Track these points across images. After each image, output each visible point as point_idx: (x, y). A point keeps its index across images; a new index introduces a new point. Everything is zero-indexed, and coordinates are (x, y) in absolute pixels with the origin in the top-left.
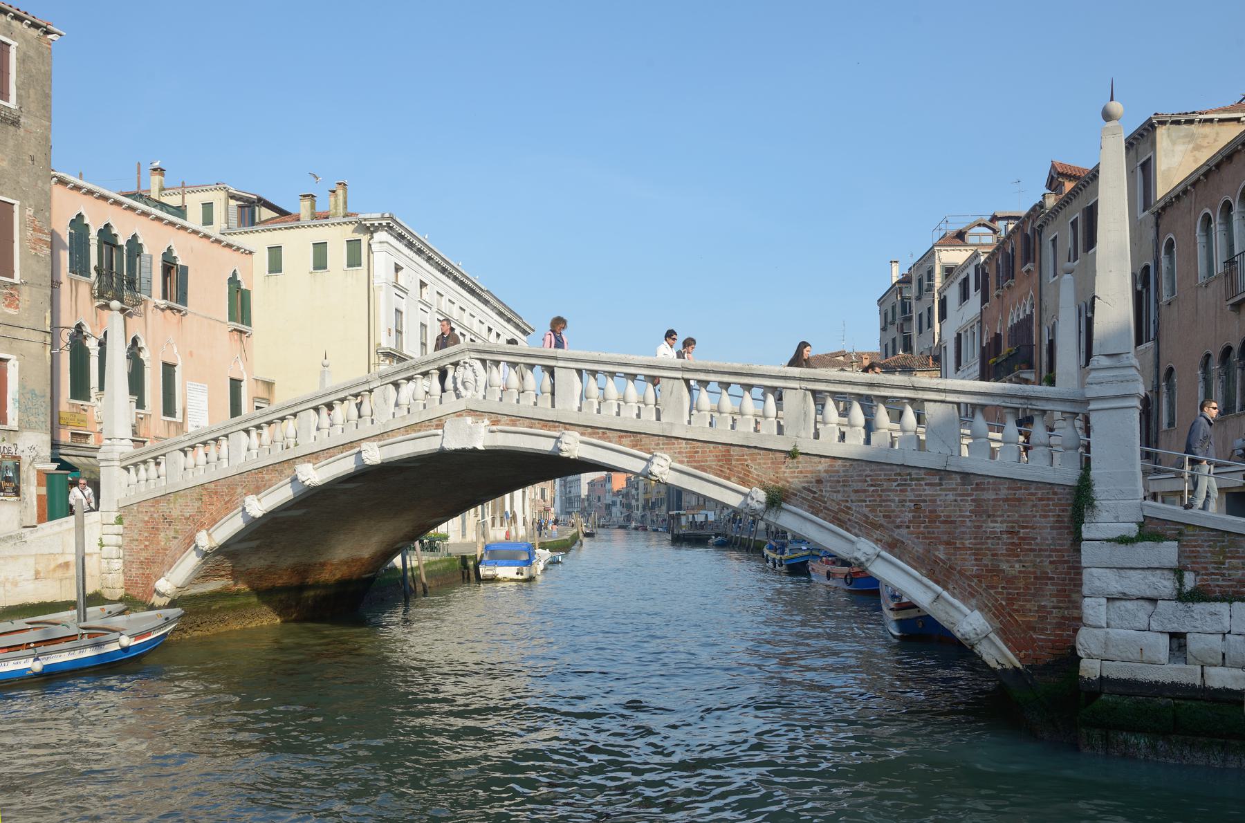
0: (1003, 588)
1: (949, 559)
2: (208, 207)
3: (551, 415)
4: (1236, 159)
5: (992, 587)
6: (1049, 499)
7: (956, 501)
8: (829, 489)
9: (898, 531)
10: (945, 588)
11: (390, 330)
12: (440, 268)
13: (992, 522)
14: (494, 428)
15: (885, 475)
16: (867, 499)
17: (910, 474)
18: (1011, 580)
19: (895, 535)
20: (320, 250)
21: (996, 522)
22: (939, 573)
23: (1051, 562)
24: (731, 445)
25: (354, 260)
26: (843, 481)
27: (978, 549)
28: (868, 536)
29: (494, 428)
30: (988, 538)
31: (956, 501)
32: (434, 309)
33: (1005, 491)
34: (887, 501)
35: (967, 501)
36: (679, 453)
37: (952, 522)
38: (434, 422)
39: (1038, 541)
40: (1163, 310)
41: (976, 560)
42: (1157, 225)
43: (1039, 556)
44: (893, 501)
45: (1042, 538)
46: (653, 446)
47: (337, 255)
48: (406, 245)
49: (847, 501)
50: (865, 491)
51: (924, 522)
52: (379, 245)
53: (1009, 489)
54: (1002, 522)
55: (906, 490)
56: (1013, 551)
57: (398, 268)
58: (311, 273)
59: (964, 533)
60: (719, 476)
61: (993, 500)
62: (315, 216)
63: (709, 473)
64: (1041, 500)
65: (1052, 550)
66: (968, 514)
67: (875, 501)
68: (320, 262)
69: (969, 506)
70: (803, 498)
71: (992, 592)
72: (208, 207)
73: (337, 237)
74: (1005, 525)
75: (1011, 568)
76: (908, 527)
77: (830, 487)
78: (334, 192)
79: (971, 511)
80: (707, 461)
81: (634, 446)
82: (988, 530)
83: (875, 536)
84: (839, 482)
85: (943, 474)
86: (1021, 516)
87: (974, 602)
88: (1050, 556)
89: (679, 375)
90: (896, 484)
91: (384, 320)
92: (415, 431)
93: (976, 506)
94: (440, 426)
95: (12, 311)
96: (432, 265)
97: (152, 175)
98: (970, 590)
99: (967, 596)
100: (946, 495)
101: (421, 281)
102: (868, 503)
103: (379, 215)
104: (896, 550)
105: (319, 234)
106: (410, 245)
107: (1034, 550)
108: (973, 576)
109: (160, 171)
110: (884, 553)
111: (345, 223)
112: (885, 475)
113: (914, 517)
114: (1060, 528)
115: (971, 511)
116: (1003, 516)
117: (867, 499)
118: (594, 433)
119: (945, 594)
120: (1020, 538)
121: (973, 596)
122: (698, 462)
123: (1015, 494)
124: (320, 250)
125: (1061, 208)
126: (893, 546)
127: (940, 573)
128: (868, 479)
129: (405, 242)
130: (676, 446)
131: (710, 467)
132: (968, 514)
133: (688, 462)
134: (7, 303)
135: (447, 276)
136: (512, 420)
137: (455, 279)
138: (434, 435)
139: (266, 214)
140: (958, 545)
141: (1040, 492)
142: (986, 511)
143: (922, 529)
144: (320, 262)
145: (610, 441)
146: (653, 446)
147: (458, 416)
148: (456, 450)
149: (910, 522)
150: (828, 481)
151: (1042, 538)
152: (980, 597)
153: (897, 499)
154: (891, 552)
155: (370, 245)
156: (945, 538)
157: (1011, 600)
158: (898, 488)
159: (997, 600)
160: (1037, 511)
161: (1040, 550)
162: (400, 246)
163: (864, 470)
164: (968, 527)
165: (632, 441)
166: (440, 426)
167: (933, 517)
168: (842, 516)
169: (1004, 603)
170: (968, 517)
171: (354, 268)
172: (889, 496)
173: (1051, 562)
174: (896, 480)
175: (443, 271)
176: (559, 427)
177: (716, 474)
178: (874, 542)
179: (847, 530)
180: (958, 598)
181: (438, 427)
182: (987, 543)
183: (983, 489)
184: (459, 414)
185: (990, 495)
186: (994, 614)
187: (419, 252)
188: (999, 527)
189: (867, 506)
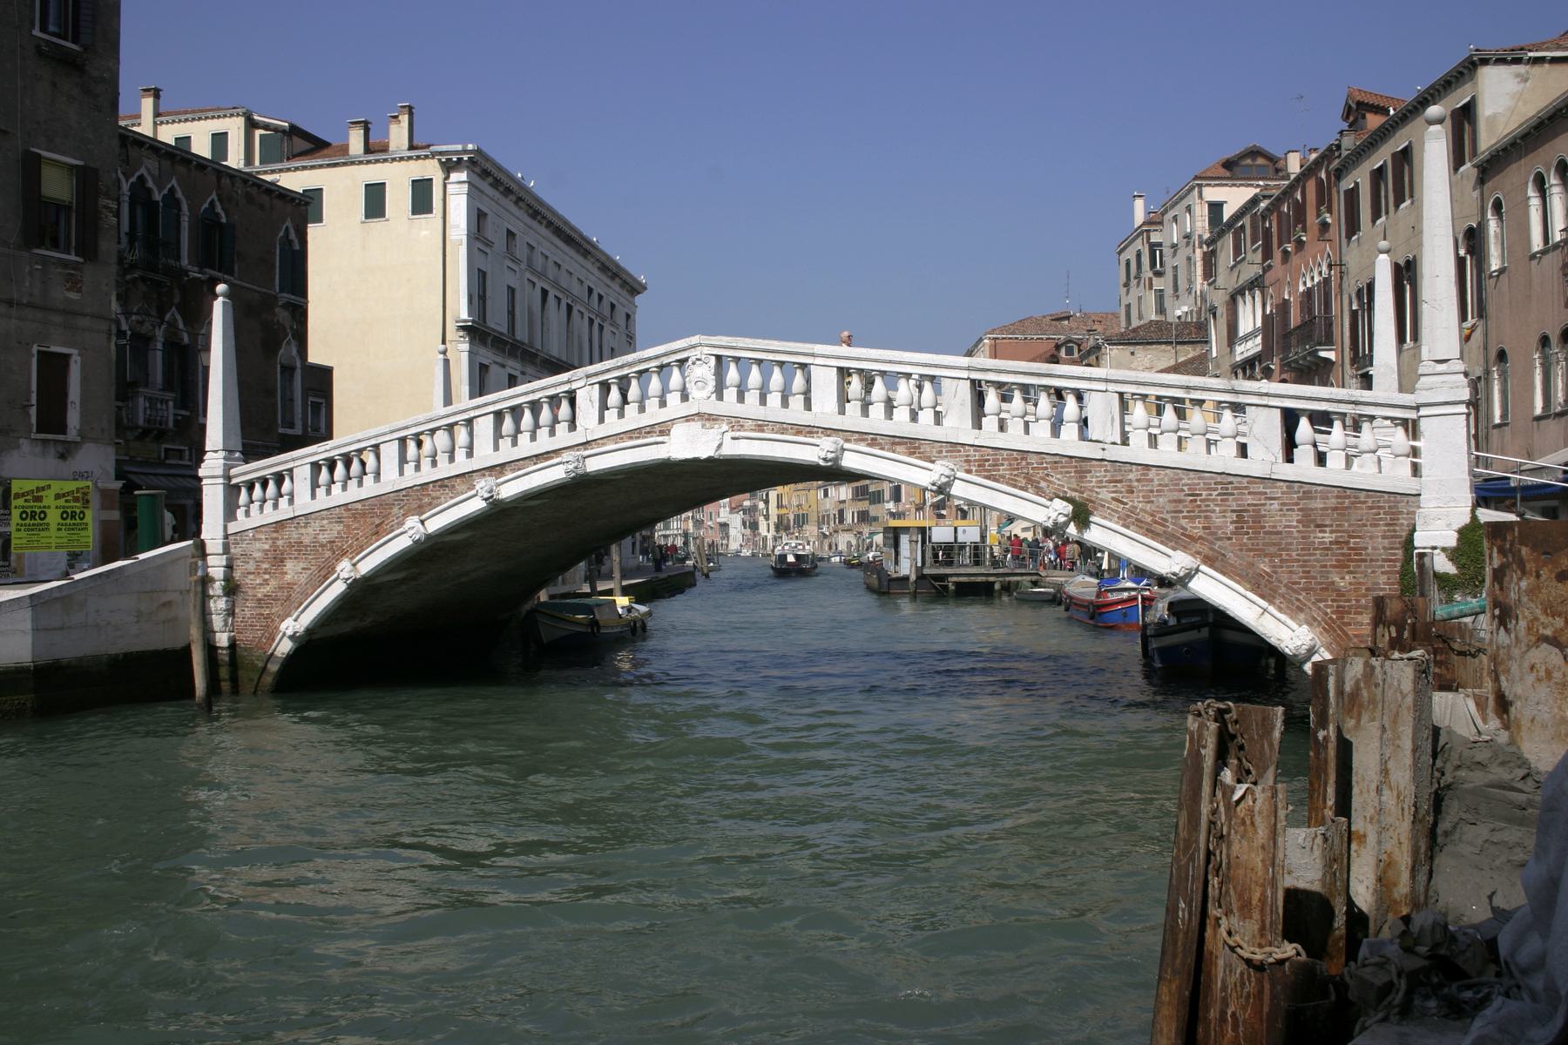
0: (1332, 601)
1: (1275, 572)
3: (805, 418)
5: (1320, 601)
6: (1379, 507)
7: (1281, 510)
8: (1141, 499)
9: (1219, 543)
10: (1271, 602)
12: (530, 211)
13: (1320, 532)
14: (737, 434)
15: (1204, 484)
16: (1185, 510)
17: (1231, 483)
19: (1216, 547)
21: (1325, 532)
22: (1262, 586)
23: (1382, 573)
24: (1028, 452)
26: (1157, 491)
27: (1304, 561)
28: (1185, 548)
29: (737, 434)
30: (1315, 549)
31: (1281, 510)
33: (1333, 500)
34: (1207, 511)
35: (1293, 510)
36: (968, 461)
37: (1280, 533)
38: (657, 428)
39: (1369, 551)
41: (1304, 572)
43: (1370, 567)
44: (1214, 511)
45: (1374, 548)
46: (935, 454)
47: (398, 199)
48: (491, 185)
49: (1162, 513)
50: (1180, 501)
51: (1248, 533)
53: (1338, 497)
54: (1332, 532)
55: (1227, 500)
56: (1341, 566)
58: (363, 223)
59: (1291, 544)
60: (1015, 486)
61: (1322, 509)
62: (368, 150)
63: (1002, 483)
64: (1371, 508)
65: (1384, 560)
66: (1295, 524)
67: (1193, 512)
69: (1295, 517)
70: (1113, 510)
71: (1322, 605)
73: (398, 178)
74: (1334, 535)
76: (1230, 539)
77: (1143, 497)
78: (396, 117)
79: (1298, 521)
80: (999, 470)
81: (911, 454)
82: (1316, 540)
83: (1194, 550)
84: (1152, 491)
86: (1350, 525)
87: (1302, 616)
88: (1383, 566)
89: (965, 374)
90: (1216, 493)
92: (631, 438)
93: (1303, 516)
95: (73, 296)
96: (520, 208)
97: (143, 97)
98: (1297, 603)
99: (1294, 609)
100: (1271, 504)
101: (508, 231)
102: (1185, 514)
103: (459, 147)
104: (1217, 564)
105: (374, 173)
107: (1365, 561)
108: (1304, 589)
109: (157, 94)
110: (1203, 568)
112: (1204, 484)
113: (1236, 528)
114: (1392, 537)
115: (1298, 521)
116: (1331, 526)
117: (1185, 510)
118: (862, 440)
119: (1271, 609)
120: (1350, 549)
121: (1301, 610)
122: (989, 471)
123: (1344, 503)
125: (1363, 150)
127: (1266, 586)
128: (1185, 488)
129: (490, 180)
130: (962, 453)
131: (1003, 477)
132: (1295, 524)
133: (976, 471)
134: (68, 285)
136: (760, 426)
137: (550, 224)
138: (657, 443)
140: (1284, 557)
141: (1370, 500)
142: (1314, 521)
143: (1245, 541)
145: (882, 449)
146: (935, 454)
147: (687, 421)
148: (686, 461)
149: (1232, 533)
150: (1140, 491)
151: (1374, 548)
152: (1308, 610)
153: (1217, 509)
154: (1211, 566)
156: (1272, 549)
157: (1341, 612)
158: (1219, 498)
159: (1326, 614)
160: (1367, 520)
161: (1372, 560)
163: (1181, 479)
164: (1295, 538)
165: (908, 449)
168: (1159, 528)
169: (1334, 617)
170: (1295, 527)
172: (1209, 506)
173: (1382, 573)
174: (1215, 490)
176: (817, 433)
177: (1008, 484)
178: (1191, 555)
179: (1162, 543)
180: (1285, 613)
181: (662, 433)
182: (1315, 554)
183: (1311, 498)
184: (688, 418)
186: (1324, 628)
187: (508, 191)
189: (1184, 517)
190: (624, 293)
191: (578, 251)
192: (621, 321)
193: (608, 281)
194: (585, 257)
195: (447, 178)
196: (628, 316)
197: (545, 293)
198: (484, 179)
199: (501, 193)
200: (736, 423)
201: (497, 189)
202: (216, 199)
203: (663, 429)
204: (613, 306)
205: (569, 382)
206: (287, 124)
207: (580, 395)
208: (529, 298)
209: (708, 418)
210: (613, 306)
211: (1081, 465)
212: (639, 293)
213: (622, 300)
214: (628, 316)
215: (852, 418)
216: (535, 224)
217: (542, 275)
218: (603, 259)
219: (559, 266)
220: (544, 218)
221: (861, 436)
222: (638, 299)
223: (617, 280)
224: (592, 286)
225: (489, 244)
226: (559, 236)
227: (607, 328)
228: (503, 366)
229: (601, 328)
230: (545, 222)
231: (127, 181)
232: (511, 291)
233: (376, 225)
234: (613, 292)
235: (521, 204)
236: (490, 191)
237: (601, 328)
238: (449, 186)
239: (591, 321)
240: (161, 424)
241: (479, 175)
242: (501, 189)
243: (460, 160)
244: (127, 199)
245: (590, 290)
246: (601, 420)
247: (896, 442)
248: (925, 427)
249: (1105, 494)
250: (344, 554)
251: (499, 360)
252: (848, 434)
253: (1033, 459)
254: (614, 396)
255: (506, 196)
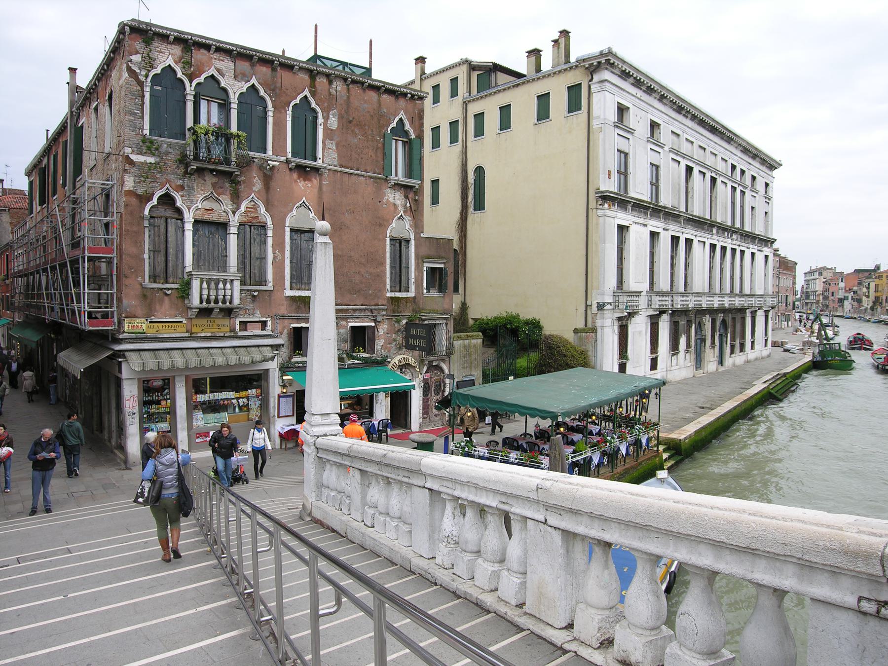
2: (454, 81)
11: (609, 172)
20: (544, 99)
25: (574, 105)
32: (666, 148)
48: (633, 84)
52: (597, 85)
57: (622, 110)
58: (536, 124)
68: (543, 114)
72: (454, 81)
91: (608, 161)
96: (666, 104)
105: (540, 88)
106: (638, 83)
111: (565, 70)
124: (544, 99)
129: (631, 80)
135: (684, 115)
137: (694, 118)
139: (502, 78)
144: (543, 114)
155: (589, 87)
162: (626, 85)
171: (574, 113)
175: (680, 110)
187: (650, 90)
190: (764, 168)
191: (722, 139)
192: (760, 186)
193: (750, 161)
194: (729, 143)
195: (591, 80)
196: (767, 185)
197: (689, 170)
198: (626, 80)
199: (644, 91)
201: (641, 89)
202: (309, 95)
204: (754, 178)
206: (491, 64)
208: (673, 174)
210: (754, 178)
212: (776, 168)
213: (761, 173)
214: (767, 185)
216: (680, 118)
217: (684, 156)
218: (744, 144)
219: (705, 149)
220: (688, 112)
222: (775, 173)
223: (757, 159)
224: (735, 164)
225: (631, 131)
226: (704, 127)
227: (748, 193)
228: (645, 225)
229: (743, 193)
230: (689, 116)
231: (191, 83)
232: (656, 167)
233: (545, 125)
234: (753, 168)
235: (664, 101)
236: (633, 90)
237: (743, 193)
238: (592, 87)
239: (734, 189)
240: (224, 302)
241: (619, 76)
242: (644, 88)
243: (599, 63)
244: (192, 98)
245: (734, 167)
251: (641, 221)
255: (650, 95)
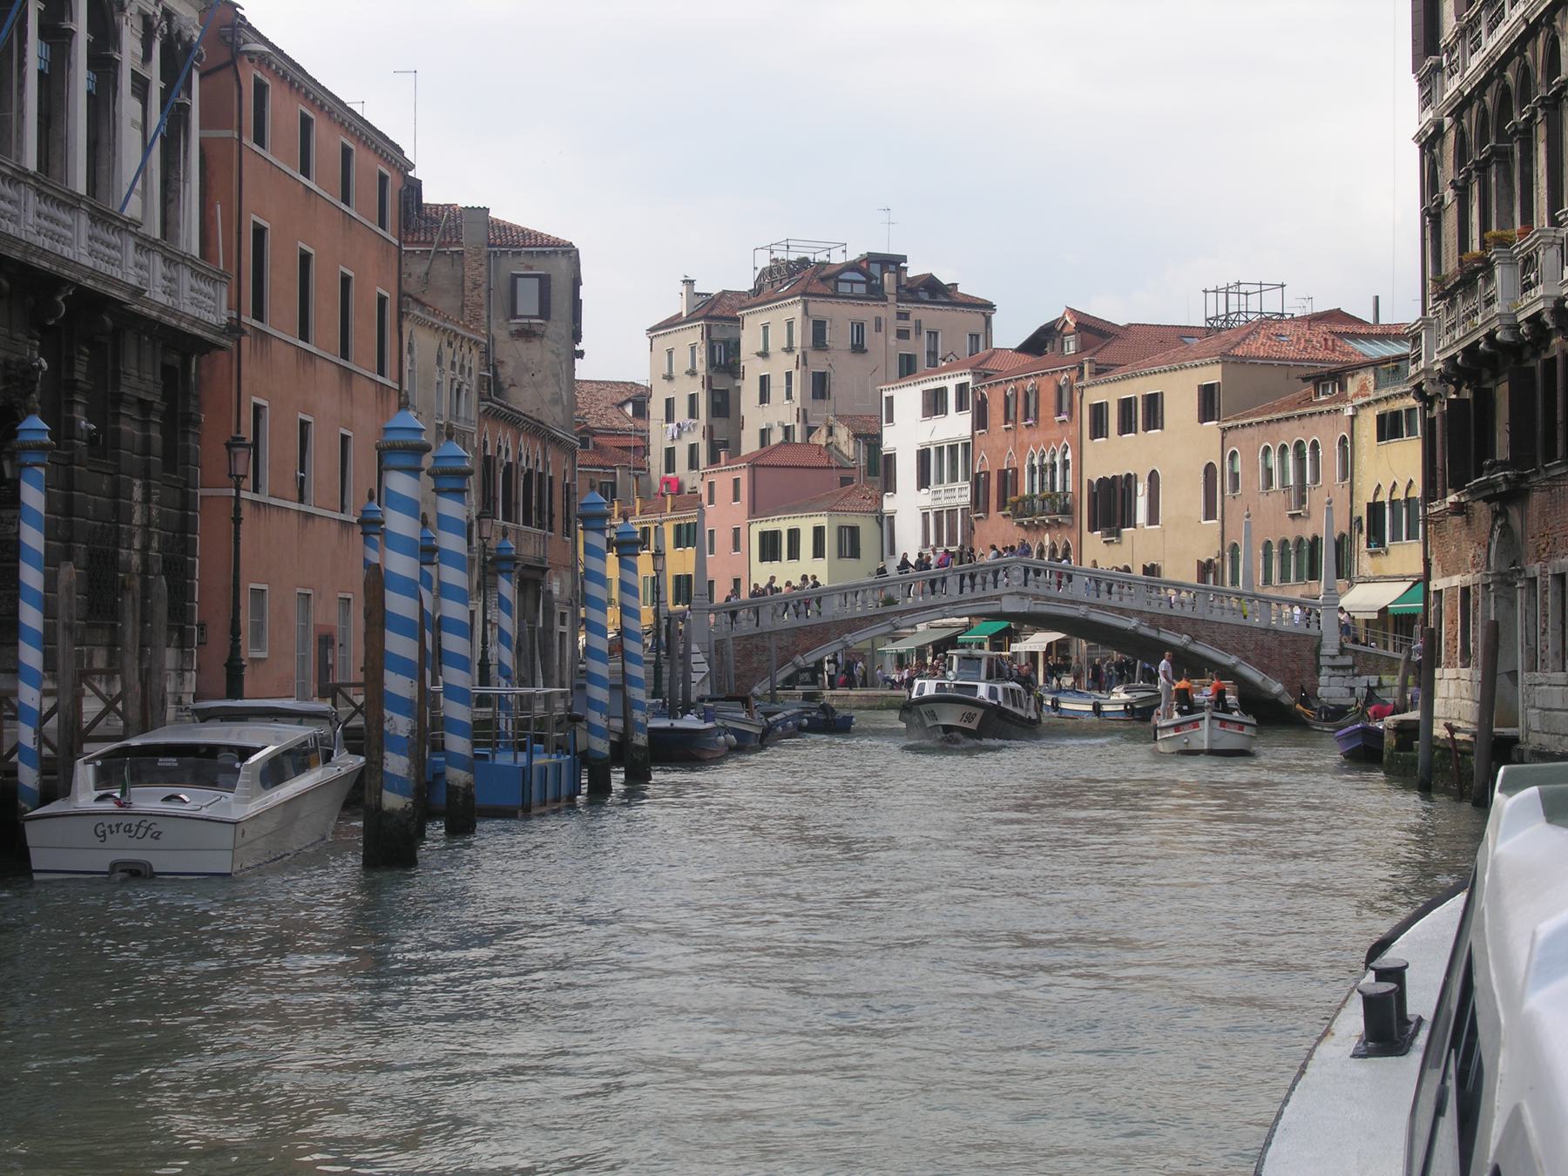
4: (1291, 422)
18: (1291, 671)
22: (1265, 669)
40: (1227, 501)
42: (1223, 438)
69: (1277, 643)
75: (1293, 666)
85: (1267, 630)
94: (1000, 600)
99: (1276, 678)
126: (1247, 659)
166: (1000, 600)
167: (1263, 647)
185: (1284, 639)
188: (1288, 651)
200: (1036, 597)
203: (998, 598)
205: (943, 573)
207: (948, 580)
209: (1023, 595)
211: (1194, 621)
215: (1093, 599)
221: (1098, 606)
246: (961, 592)
247: (1113, 609)
248: (1126, 603)
249: (1203, 633)
250: (796, 653)
252: (1091, 605)
253: (1174, 619)
254: (967, 581)
